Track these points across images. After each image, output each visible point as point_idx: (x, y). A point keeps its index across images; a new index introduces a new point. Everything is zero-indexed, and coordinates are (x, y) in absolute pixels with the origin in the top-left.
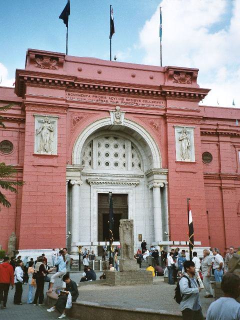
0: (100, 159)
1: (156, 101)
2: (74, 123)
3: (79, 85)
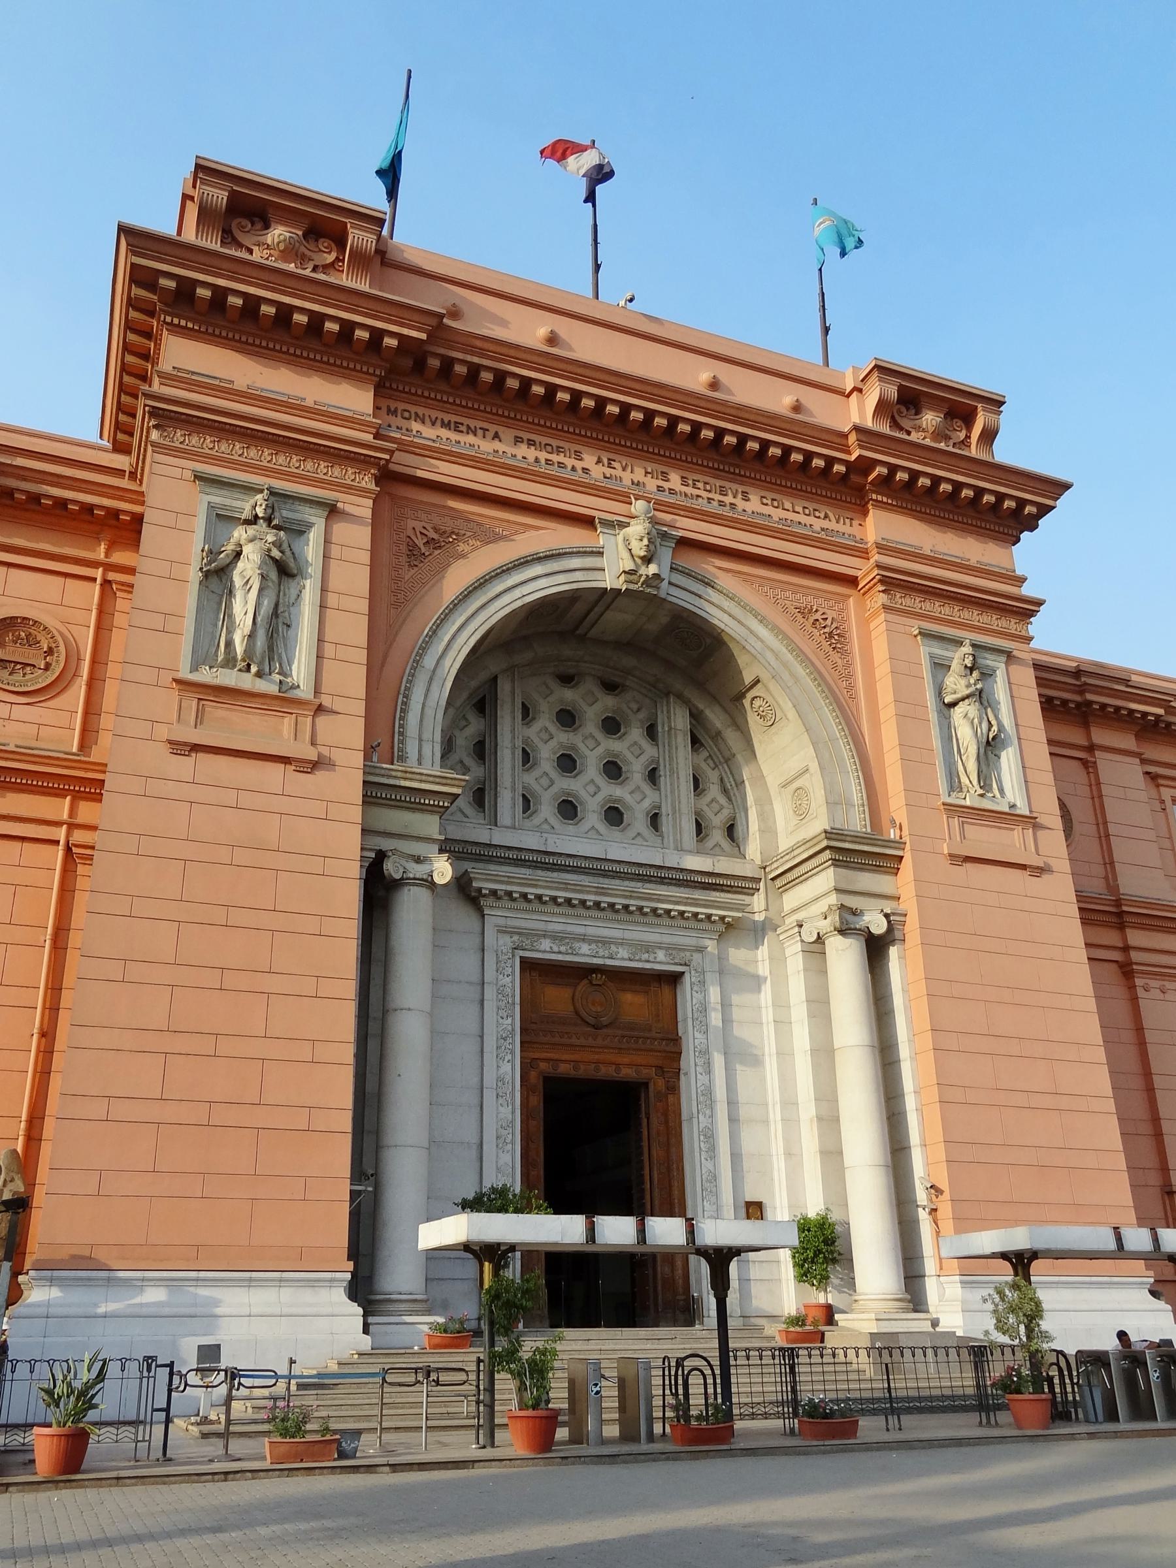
0: (530, 779)
1: (824, 510)
2: (414, 555)
3: (448, 364)
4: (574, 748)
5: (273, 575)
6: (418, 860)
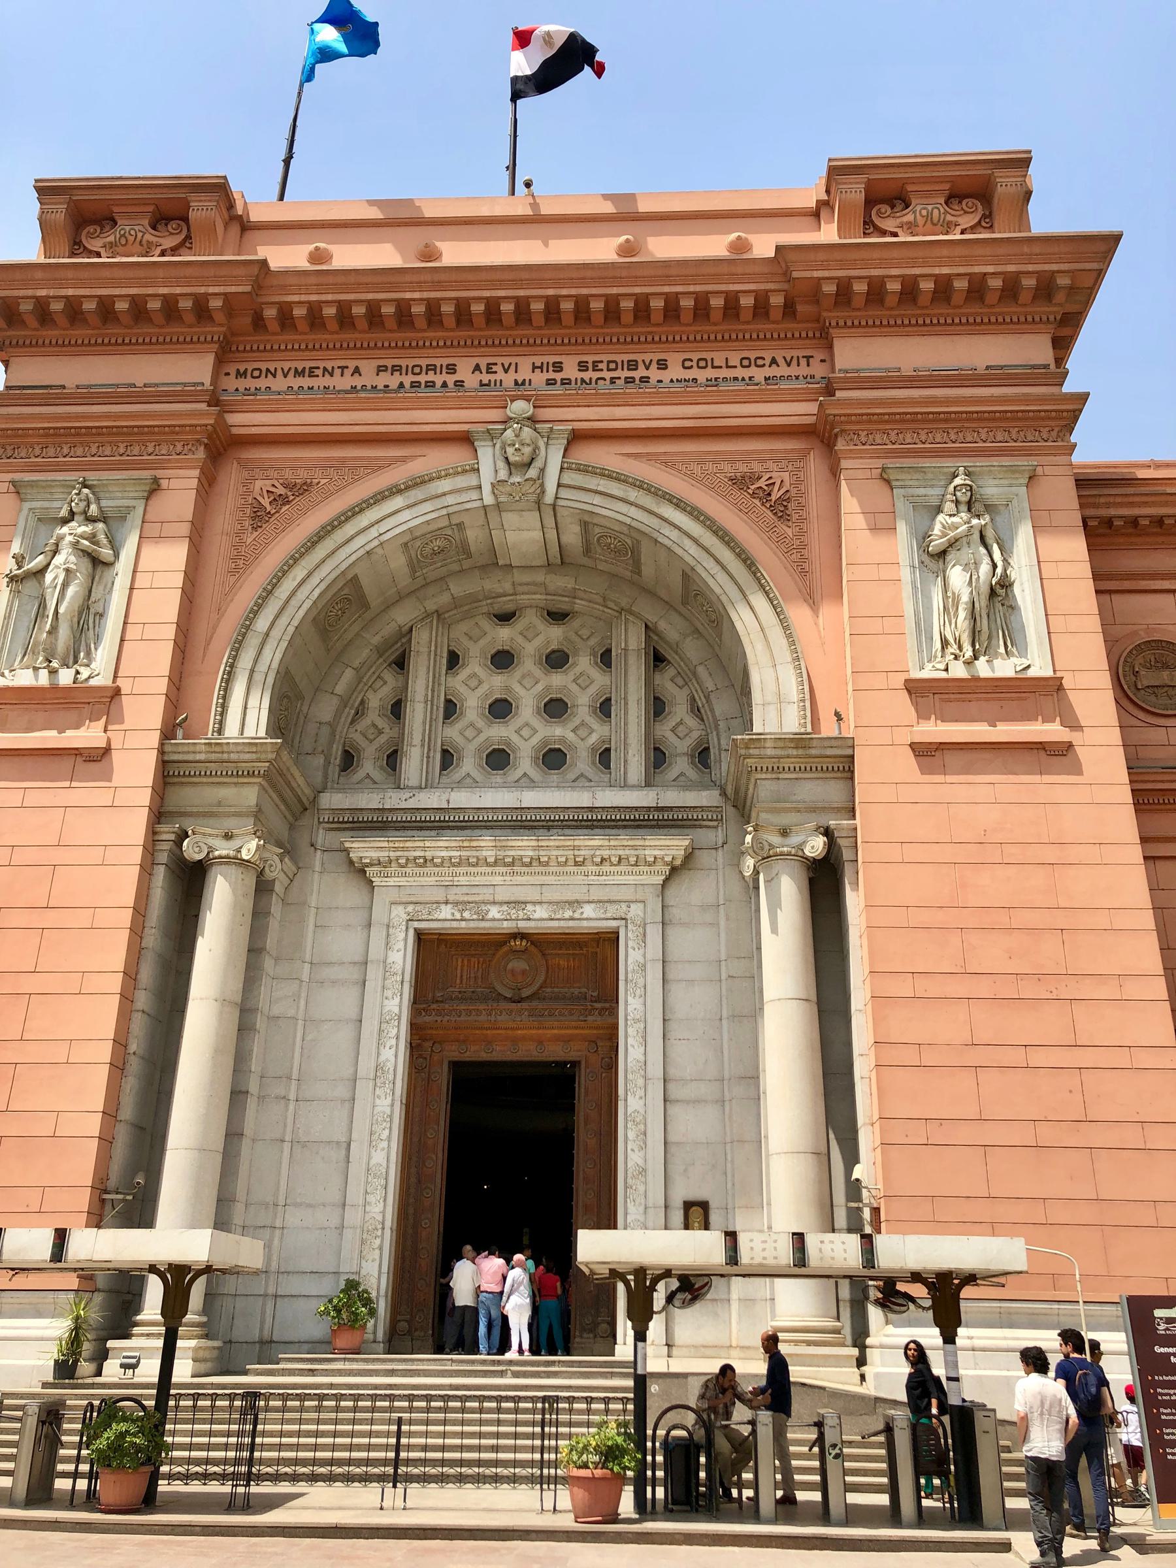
0: (453, 732)
2: (259, 517)
4: (508, 689)
5: (86, 564)
6: (228, 836)
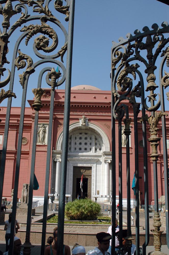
0: (76, 146)
3: (61, 105)
5: (43, 132)
